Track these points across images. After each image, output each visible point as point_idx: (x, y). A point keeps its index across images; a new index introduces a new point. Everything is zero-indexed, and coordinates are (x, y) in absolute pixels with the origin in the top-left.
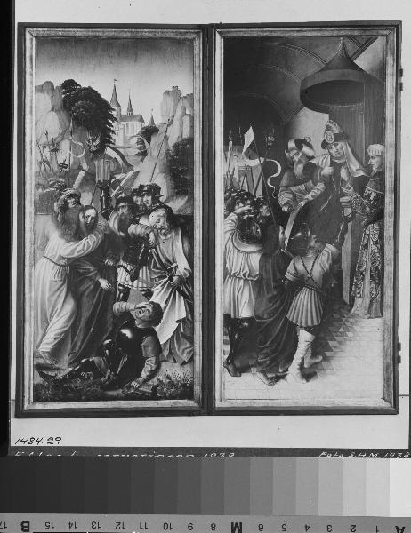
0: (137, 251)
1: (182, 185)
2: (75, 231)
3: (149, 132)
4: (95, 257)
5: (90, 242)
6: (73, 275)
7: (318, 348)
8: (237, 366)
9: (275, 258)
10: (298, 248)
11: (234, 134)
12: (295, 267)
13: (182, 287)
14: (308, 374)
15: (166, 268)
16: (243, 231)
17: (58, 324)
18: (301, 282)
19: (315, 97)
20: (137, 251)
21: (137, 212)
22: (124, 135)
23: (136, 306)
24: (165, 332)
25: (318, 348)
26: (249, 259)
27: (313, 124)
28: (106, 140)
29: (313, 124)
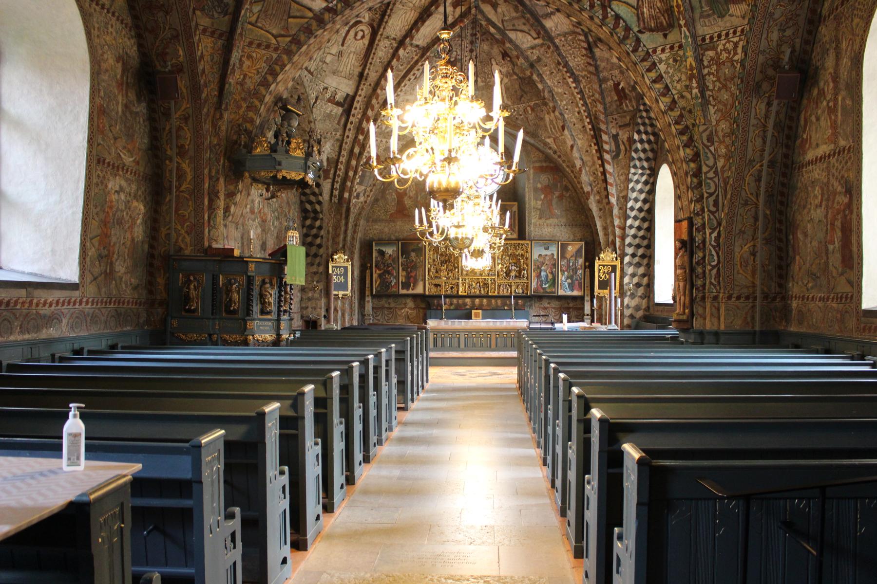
0: (388, 272)
1: (394, 263)
2: (380, 270)
3: (390, 256)
4: (383, 273)
5: (382, 271)
6: (380, 276)
7: (414, 286)
8: (403, 288)
9: (408, 273)
10: (411, 272)
11: (402, 256)
12: (411, 274)
13: (395, 277)
14: (413, 290)
15: (392, 275)
16: (403, 270)
17: (378, 283)
18: (411, 276)
19: (413, 251)
20: (388, 272)
21: (389, 267)
22: (387, 256)
23: (389, 280)
24: (393, 284)
25: (414, 286)
26: (404, 273)
27: (413, 254)
28: (384, 256)
29: (413, 254)
